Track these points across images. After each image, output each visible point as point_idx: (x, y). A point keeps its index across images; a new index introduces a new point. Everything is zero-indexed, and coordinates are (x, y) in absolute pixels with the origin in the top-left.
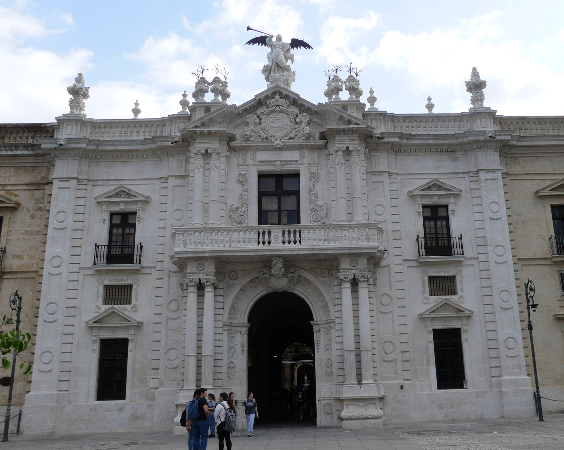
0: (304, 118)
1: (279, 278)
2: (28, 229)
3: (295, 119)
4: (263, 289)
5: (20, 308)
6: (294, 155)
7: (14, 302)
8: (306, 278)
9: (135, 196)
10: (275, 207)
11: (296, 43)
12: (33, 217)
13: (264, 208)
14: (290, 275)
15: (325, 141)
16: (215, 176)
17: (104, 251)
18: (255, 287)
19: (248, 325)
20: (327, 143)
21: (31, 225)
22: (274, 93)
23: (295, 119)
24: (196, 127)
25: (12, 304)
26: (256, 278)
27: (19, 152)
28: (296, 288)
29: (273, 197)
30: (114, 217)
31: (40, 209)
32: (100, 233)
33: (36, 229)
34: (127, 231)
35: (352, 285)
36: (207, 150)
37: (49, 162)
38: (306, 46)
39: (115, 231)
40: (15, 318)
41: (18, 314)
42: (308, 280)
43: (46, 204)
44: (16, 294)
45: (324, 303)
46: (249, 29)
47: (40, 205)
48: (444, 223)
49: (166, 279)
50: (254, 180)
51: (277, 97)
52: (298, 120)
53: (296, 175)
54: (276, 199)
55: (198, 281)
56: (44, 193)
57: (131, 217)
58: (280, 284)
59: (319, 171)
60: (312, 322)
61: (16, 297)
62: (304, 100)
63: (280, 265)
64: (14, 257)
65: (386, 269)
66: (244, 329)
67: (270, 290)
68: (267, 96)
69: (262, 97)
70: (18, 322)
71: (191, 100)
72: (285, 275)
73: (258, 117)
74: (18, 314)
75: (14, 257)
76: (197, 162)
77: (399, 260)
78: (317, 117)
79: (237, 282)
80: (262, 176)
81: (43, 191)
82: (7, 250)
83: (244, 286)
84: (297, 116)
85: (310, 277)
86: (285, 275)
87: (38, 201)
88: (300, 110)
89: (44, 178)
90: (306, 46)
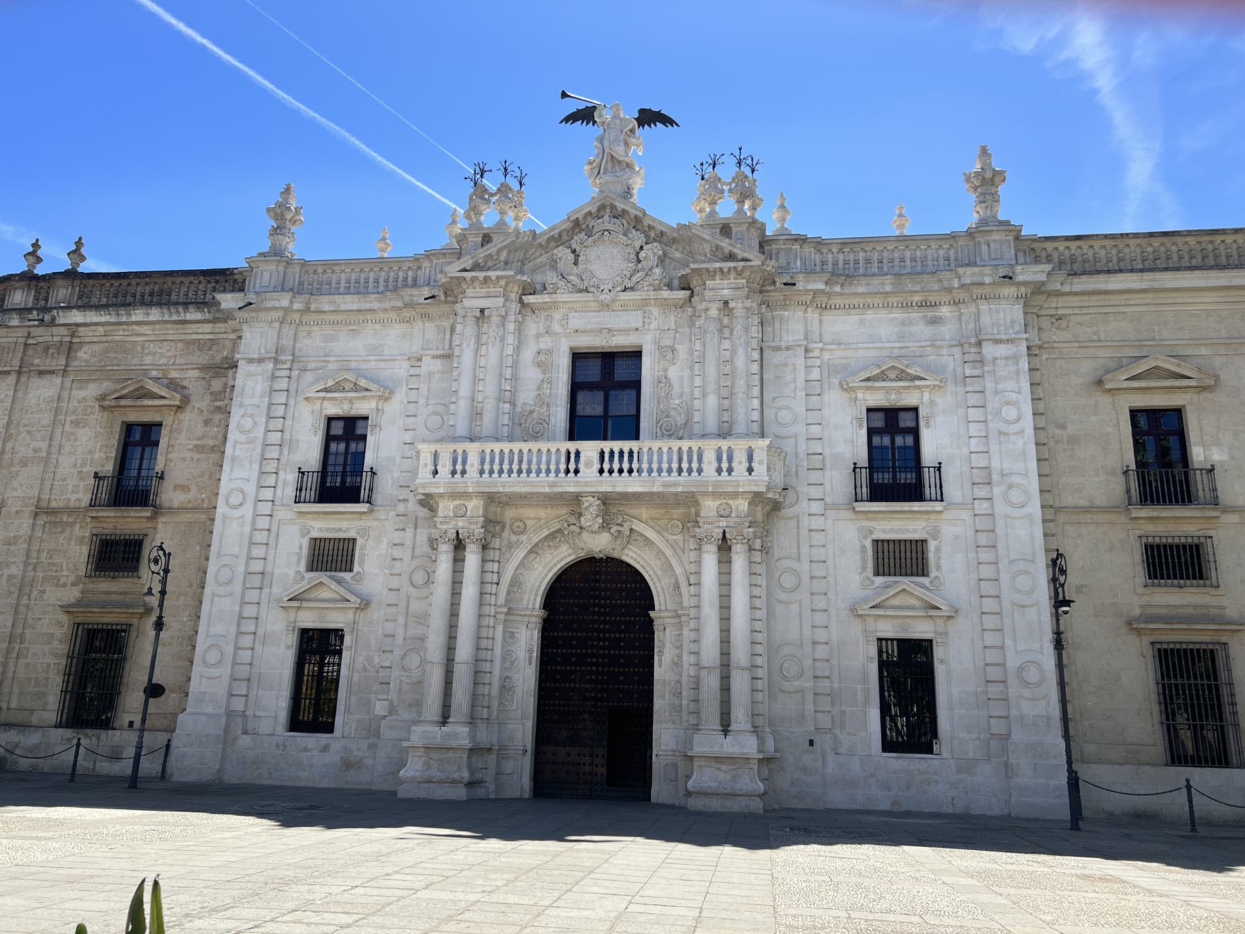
0: (652, 252)
1: (595, 532)
2: (199, 442)
3: (637, 254)
4: (570, 551)
5: (166, 571)
6: (634, 319)
7: (156, 561)
8: (642, 535)
9: (367, 390)
10: (599, 410)
11: (648, 118)
12: (207, 422)
13: (580, 411)
14: (615, 529)
15: (689, 292)
16: (492, 354)
17: (312, 481)
18: (556, 547)
19: (542, 613)
20: (692, 295)
21: (204, 436)
22: (602, 208)
23: (637, 254)
24: (465, 270)
25: (152, 565)
26: (557, 531)
27: (189, 317)
28: (626, 551)
29: (596, 392)
30: (334, 423)
31: (219, 409)
32: (309, 451)
33: (211, 442)
34: (353, 446)
35: (720, 548)
36: (482, 311)
37: (234, 331)
38: (667, 121)
39: (333, 446)
40: (157, 588)
41: (164, 582)
42: (647, 539)
43: (226, 402)
44: (161, 548)
45: (673, 581)
46: (564, 95)
47: (218, 404)
48: (909, 440)
49: (410, 531)
50: (564, 362)
51: (606, 217)
52: (642, 254)
53: (636, 355)
54: (600, 395)
55: (454, 536)
56: (226, 384)
57: (360, 423)
58: (599, 543)
59: (677, 346)
60: (652, 614)
61: (161, 553)
62: (654, 220)
63: (594, 510)
64: (176, 487)
65: (793, 523)
66: (533, 619)
67: (582, 555)
68: (590, 213)
69: (580, 216)
70: (163, 593)
71: (462, 224)
72: (605, 526)
73: (574, 251)
74: (164, 582)
75: (176, 487)
76: (467, 330)
77: (816, 507)
78: (677, 250)
79: (523, 538)
80: (578, 358)
81: (224, 380)
82: (166, 476)
83: (536, 545)
84: (642, 248)
85: (650, 533)
86: (605, 526)
87: (216, 396)
88: (647, 237)
89: (226, 358)
90: (667, 121)
